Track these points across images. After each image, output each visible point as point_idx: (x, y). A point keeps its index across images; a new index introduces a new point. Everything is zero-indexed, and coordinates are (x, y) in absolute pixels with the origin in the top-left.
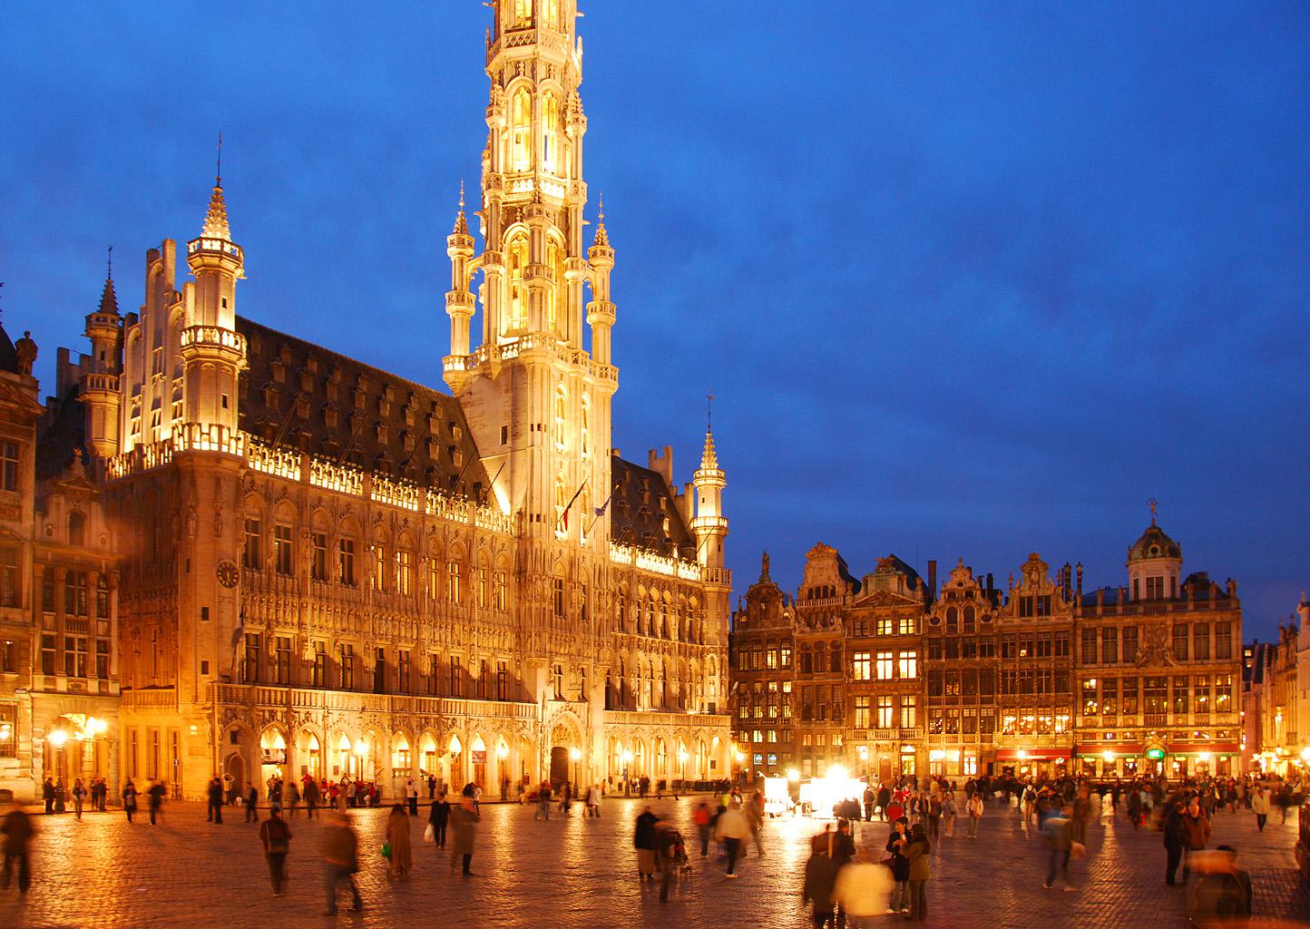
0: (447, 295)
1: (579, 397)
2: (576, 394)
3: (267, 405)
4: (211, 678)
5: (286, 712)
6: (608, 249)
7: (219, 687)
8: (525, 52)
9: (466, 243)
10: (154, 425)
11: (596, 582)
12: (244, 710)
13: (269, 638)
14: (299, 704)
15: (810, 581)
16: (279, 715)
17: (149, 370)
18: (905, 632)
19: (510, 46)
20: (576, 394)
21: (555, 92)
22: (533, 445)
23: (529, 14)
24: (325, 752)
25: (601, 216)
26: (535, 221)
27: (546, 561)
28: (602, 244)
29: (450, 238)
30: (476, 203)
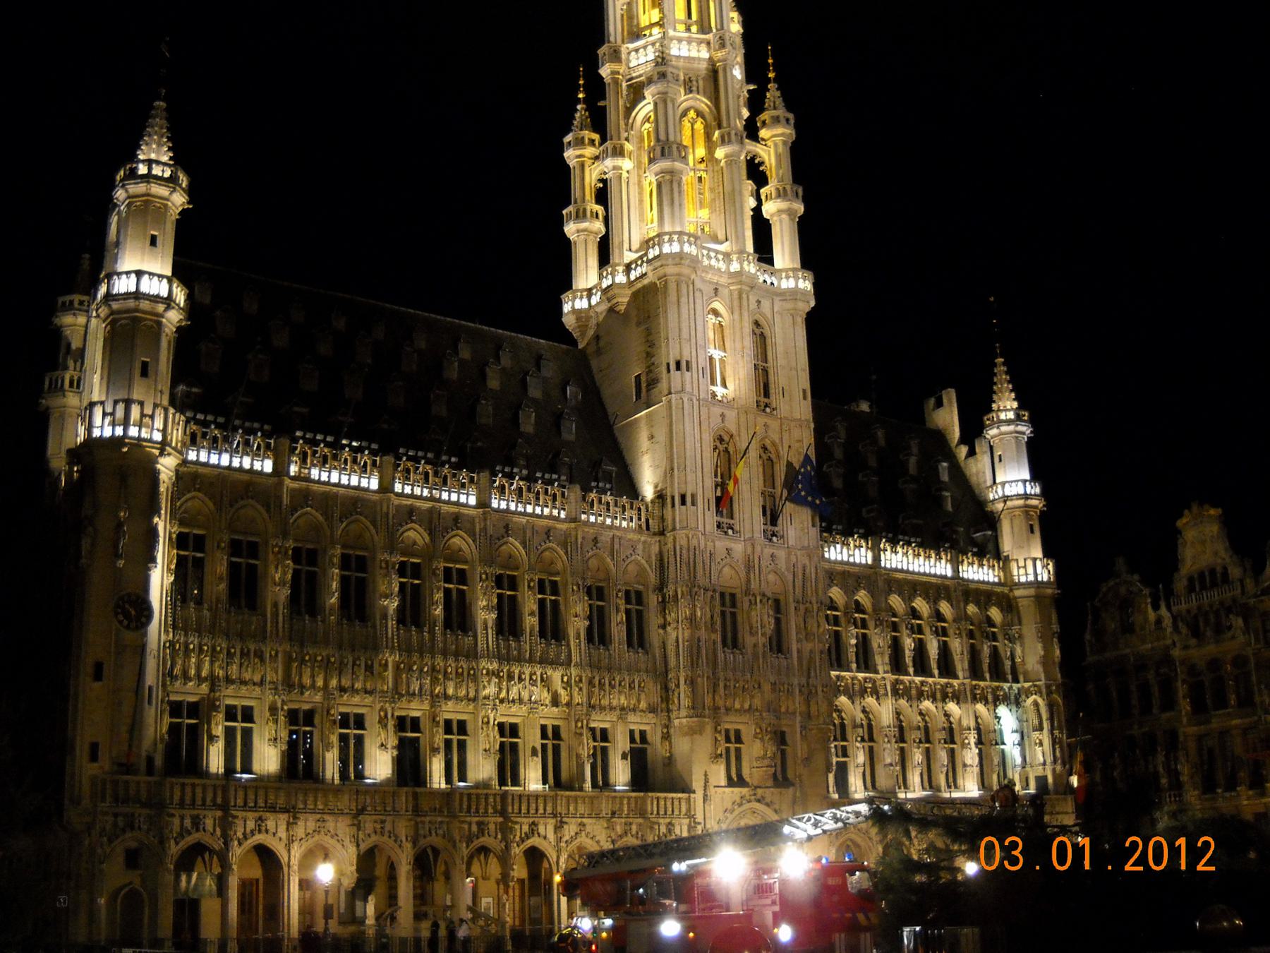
0: (564, 212)
2: (741, 314)
6: (781, 112)
9: (587, 141)
15: (1189, 562)
16: (209, 823)
28: (775, 108)
30: (597, 88)
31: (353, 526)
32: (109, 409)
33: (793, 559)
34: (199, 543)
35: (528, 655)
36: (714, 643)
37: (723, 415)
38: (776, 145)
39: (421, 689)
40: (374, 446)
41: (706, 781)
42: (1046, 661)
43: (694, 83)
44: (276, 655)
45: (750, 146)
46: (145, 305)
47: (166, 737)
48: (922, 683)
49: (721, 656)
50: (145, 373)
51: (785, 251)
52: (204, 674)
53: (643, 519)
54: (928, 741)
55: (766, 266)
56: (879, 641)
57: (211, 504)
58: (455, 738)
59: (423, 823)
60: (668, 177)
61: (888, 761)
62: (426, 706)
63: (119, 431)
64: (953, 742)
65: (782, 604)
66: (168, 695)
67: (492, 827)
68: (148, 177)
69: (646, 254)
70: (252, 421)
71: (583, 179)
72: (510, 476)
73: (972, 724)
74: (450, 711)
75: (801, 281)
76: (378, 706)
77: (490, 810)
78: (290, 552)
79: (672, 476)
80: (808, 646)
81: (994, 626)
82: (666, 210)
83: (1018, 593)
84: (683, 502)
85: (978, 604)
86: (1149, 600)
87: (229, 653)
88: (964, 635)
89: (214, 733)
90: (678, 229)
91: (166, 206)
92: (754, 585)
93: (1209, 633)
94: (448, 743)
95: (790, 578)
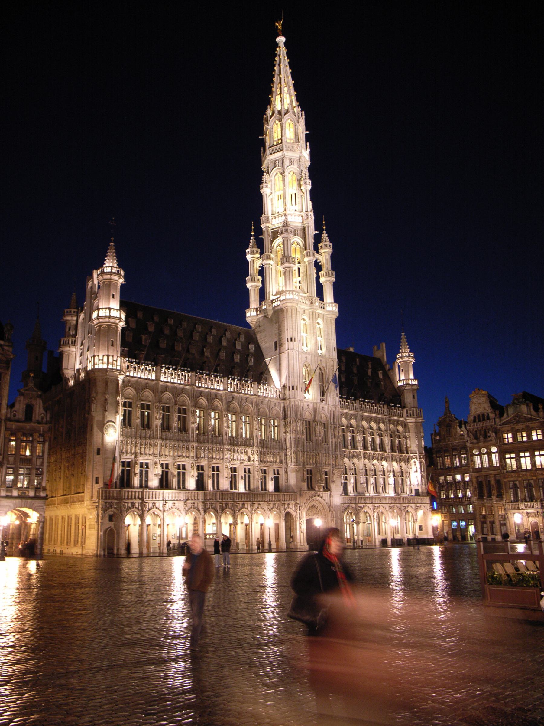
0: (247, 278)
1: (315, 321)
2: (313, 320)
3: (143, 343)
4: (100, 486)
5: (141, 503)
6: (328, 243)
7: (102, 491)
8: (278, 155)
12: (117, 503)
13: (136, 463)
15: (473, 411)
16: (137, 505)
17: (86, 333)
18: (509, 434)
19: (271, 154)
20: (313, 320)
21: (295, 171)
22: (288, 349)
23: (280, 137)
25: (324, 228)
28: (325, 241)
29: (247, 251)
30: (259, 231)
31: (181, 398)
32: (101, 358)
33: (330, 408)
34: (130, 405)
35: (240, 443)
36: (303, 439)
37: (306, 357)
38: (325, 255)
39: (204, 456)
42: (419, 446)
43: (297, 232)
44: (157, 445)
45: (317, 256)
46: (112, 320)
47: (121, 474)
48: (374, 454)
49: (305, 443)
50: (112, 345)
51: (329, 296)
52: (133, 451)
53: (278, 394)
54: (376, 475)
55: (322, 302)
56: (359, 438)
57: (134, 391)
58: (215, 473)
59: (207, 503)
60: (288, 269)
61: (362, 482)
62: (206, 461)
63: (105, 366)
64: (384, 475)
65: (326, 424)
66: (121, 459)
68: (111, 273)
69: (279, 297)
70: (148, 361)
71: (254, 266)
72: (234, 379)
73: (392, 469)
74: (215, 463)
75: (334, 307)
76: (191, 462)
77: (229, 499)
78: (162, 408)
79: (289, 379)
81: (399, 433)
82: (288, 282)
83: (408, 421)
84: (293, 389)
85: (394, 425)
86: (458, 424)
87: (141, 443)
88: (389, 436)
89: (136, 472)
90: (291, 289)
91: (117, 283)
93: (481, 438)
94: (213, 474)
95: (329, 415)
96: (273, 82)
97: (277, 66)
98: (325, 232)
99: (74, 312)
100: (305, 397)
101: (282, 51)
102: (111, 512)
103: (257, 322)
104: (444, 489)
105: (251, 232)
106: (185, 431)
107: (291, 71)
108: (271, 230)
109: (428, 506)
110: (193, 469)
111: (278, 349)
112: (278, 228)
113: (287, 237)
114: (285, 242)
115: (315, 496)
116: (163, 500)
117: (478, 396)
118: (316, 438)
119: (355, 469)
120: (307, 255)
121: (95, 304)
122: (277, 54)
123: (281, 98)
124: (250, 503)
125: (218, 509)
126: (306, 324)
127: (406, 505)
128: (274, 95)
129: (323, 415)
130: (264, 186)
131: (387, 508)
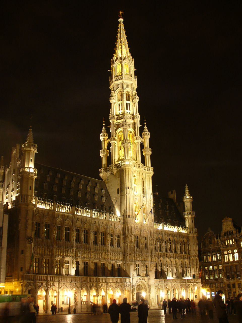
0: (100, 151)
3: (44, 188)
5: (46, 283)
6: (148, 133)
9: (105, 135)
10: (12, 196)
11: (150, 236)
14: (51, 280)
15: (224, 229)
16: (44, 284)
19: (116, 81)
24: (58, 296)
25: (145, 123)
26: (125, 127)
27: (132, 230)
28: (146, 131)
29: (101, 134)
30: (108, 124)
33: (149, 229)
40: (71, 205)
41: (133, 275)
49: (136, 249)
53: (120, 220)
59: (82, 284)
65: (147, 238)
67: (95, 285)
76: (72, 259)
80: (151, 247)
90: (128, 159)
92: (142, 235)
95: (148, 232)
96: (117, 42)
97: (119, 33)
98: (146, 126)
99: (3, 167)
100: (135, 222)
101: (122, 26)
102: (29, 288)
103: (106, 177)
104: (207, 274)
105: (103, 124)
106: (60, 240)
107: (126, 37)
108: (116, 123)
109: (200, 284)
110: (74, 263)
111: (119, 193)
112: (120, 122)
113: (126, 128)
114: (125, 131)
115: (141, 279)
116: (58, 281)
117: (227, 221)
118: (142, 246)
119: (161, 263)
120: (137, 139)
121: (18, 164)
122: (118, 27)
123: (121, 50)
124: (106, 283)
125: (89, 287)
126: (135, 179)
127: (188, 284)
128: (117, 49)
129: (145, 232)
130: (112, 99)
131: (179, 285)
